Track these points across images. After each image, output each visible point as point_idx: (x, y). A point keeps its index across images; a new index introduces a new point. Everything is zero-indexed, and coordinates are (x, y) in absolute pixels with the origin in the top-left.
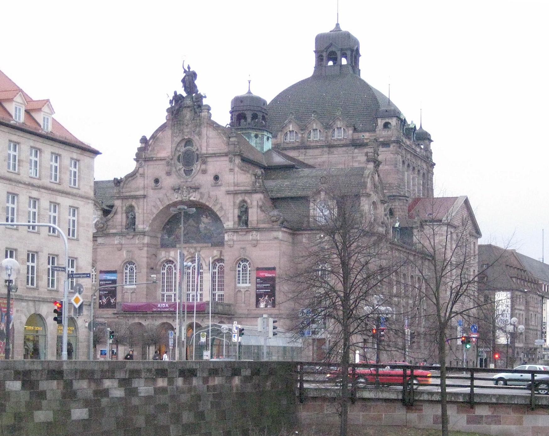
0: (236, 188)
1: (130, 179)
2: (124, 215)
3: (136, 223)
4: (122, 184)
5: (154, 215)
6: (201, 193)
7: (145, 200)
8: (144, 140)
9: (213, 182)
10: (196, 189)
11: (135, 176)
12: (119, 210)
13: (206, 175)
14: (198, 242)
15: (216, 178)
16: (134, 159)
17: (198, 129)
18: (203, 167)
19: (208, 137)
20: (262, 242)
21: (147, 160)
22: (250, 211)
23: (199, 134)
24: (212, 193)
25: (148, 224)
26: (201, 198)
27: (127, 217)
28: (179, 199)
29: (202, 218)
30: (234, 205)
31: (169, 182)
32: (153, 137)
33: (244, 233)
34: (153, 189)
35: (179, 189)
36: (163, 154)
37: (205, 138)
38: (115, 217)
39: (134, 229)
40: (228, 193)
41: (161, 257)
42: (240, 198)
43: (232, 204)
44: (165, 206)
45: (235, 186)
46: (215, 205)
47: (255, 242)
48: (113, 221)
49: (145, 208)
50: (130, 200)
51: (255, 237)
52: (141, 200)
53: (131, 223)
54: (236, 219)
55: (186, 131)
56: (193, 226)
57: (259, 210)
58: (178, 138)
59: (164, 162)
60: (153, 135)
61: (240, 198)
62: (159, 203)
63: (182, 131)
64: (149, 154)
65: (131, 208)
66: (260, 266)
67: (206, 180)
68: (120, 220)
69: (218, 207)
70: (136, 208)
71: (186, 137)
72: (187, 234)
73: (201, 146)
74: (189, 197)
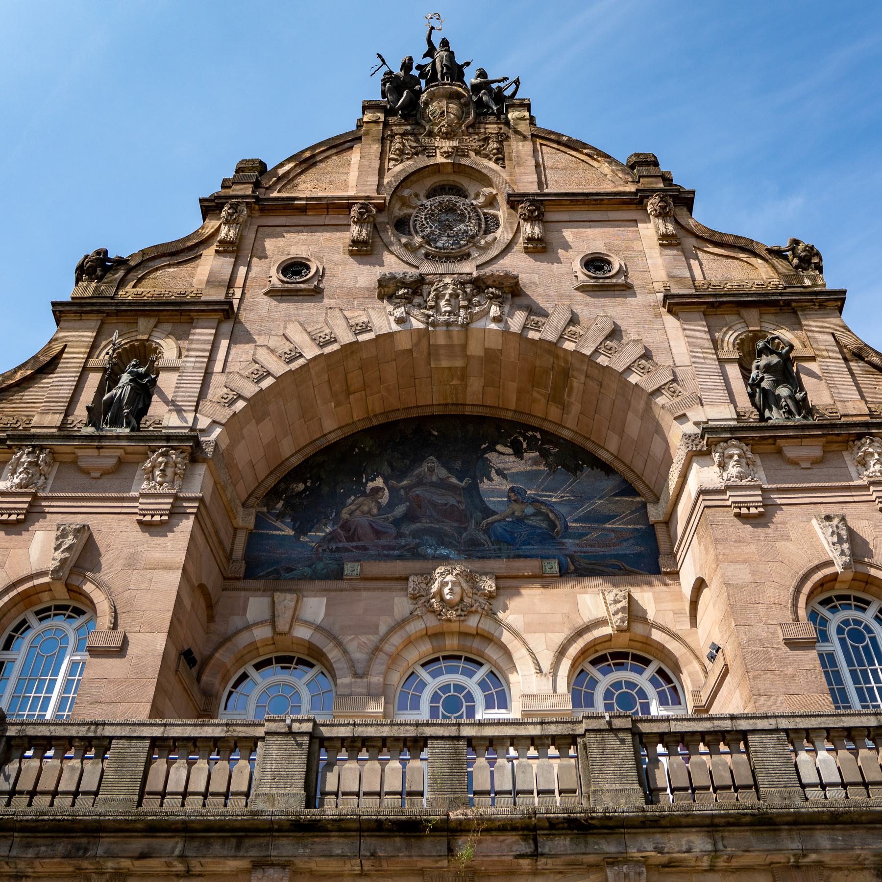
2: (94, 379)
12: (75, 357)
14: (471, 550)
24: (584, 314)
25: (224, 414)
33: (816, 451)
41: (237, 622)
49: (221, 354)
50: (144, 324)
56: (443, 484)
62: (300, 338)
68: (66, 392)
72: (410, 517)
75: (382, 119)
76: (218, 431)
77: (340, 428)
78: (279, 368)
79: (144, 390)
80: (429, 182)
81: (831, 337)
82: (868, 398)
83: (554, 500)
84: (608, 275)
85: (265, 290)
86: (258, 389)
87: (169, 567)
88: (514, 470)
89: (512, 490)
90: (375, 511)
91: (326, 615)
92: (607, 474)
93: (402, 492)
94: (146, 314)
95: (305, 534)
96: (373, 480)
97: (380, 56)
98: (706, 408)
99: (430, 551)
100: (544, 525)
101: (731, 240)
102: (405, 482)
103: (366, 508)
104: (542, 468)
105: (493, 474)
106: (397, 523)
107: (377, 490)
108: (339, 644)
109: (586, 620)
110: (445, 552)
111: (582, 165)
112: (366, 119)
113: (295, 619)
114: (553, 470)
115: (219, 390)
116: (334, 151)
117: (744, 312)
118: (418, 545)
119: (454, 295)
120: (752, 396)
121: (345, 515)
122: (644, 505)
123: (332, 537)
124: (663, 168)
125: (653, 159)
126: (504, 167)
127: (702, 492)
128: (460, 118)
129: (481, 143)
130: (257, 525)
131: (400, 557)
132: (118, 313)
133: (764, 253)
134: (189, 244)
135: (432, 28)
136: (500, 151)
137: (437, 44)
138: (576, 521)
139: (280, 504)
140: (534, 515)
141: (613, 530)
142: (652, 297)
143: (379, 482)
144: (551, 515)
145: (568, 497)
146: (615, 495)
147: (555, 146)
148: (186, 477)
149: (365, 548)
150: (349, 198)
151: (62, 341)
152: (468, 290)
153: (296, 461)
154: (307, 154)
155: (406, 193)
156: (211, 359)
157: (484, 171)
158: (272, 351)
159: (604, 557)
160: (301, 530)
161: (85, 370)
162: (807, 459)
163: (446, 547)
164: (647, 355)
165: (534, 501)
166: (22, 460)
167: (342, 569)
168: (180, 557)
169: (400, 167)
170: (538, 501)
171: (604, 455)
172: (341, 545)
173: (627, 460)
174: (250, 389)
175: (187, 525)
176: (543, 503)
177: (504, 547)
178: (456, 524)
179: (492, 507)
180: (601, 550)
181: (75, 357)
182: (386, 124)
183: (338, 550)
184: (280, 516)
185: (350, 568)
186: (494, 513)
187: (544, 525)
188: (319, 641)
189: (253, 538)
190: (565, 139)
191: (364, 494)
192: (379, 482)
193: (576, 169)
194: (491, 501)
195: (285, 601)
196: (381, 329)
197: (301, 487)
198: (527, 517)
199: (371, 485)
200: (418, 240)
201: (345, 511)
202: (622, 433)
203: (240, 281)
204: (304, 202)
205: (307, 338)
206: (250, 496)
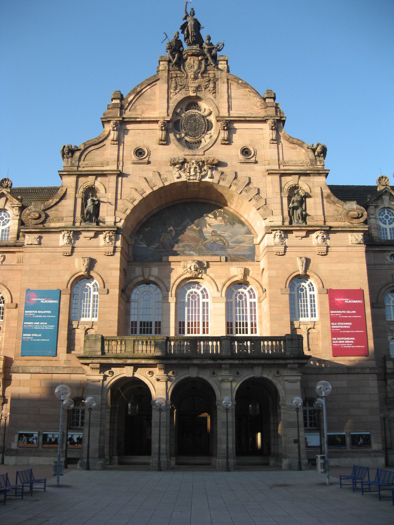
0: (282, 167)
2: (79, 201)
4: (77, 154)
7: (120, 179)
11: (101, 145)
19: (229, 97)
25: (124, 216)
27: (84, 205)
29: (207, 218)
33: (304, 234)
35: (183, 163)
38: (63, 202)
42: (290, 181)
53: (92, 215)
54: (286, 213)
58: (178, 95)
61: (290, 181)
62: (144, 185)
63: (185, 87)
65: (91, 191)
68: (72, 208)
75: (167, 69)
76: (123, 221)
77: (158, 207)
78: (139, 198)
79: (97, 207)
80: (186, 103)
82: (326, 214)
83: (225, 235)
84: (249, 157)
85: (130, 162)
86: (133, 206)
87: (116, 269)
88: (214, 224)
89: (213, 231)
90: (171, 238)
91: (158, 273)
92: (243, 226)
93: (179, 232)
95: (150, 247)
96: (170, 227)
98: (274, 216)
99: (187, 252)
100: (222, 244)
101: (295, 141)
102: (180, 228)
103: (168, 237)
104: (223, 223)
105: (207, 226)
107: (171, 231)
108: (163, 282)
109: (232, 275)
112: (160, 69)
113: (150, 275)
114: (226, 224)
115: (121, 206)
116: (149, 87)
118: (184, 250)
119: (195, 168)
120: (289, 212)
121: (161, 240)
122: (253, 238)
123: (158, 248)
124: (276, 102)
125: (273, 96)
127: (268, 246)
128: (199, 68)
129: (207, 83)
134: (100, 140)
136: (215, 88)
137: (189, 11)
138: (231, 243)
139: (141, 236)
140: (219, 240)
141: (243, 246)
142: (263, 167)
143: (171, 228)
144: (224, 241)
145: (230, 234)
146: (245, 234)
148: (116, 239)
149: (168, 251)
150: (157, 118)
151: (65, 186)
153: (145, 220)
154: (139, 89)
155: (179, 110)
156: (116, 193)
159: (239, 255)
161: (76, 199)
163: (192, 251)
164: (258, 193)
166: (65, 235)
167: (162, 259)
168: (118, 266)
169: (175, 97)
170: (221, 235)
171: (243, 219)
172: (161, 250)
173: (250, 222)
175: (118, 255)
176: (222, 236)
177: (210, 251)
178: (195, 243)
179: (206, 237)
180: (239, 253)
181: (71, 192)
182: (169, 71)
183: (160, 252)
184: (142, 240)
186: (207, 239)
187: (222, 244)
188: (157, 281)
190: (240, 82)
191: (167, 232)
192: (171, 228)
193: (243, 99)
194: (206, 235)
195: (147, 270)
196: (171, 181)
197: (147, 230)
199: (169, 229)
200: (183, 135)
201: (162, 238)
202: (248, 215)
203: (121, 158)
204: (140, 120)
206: (132, 233)
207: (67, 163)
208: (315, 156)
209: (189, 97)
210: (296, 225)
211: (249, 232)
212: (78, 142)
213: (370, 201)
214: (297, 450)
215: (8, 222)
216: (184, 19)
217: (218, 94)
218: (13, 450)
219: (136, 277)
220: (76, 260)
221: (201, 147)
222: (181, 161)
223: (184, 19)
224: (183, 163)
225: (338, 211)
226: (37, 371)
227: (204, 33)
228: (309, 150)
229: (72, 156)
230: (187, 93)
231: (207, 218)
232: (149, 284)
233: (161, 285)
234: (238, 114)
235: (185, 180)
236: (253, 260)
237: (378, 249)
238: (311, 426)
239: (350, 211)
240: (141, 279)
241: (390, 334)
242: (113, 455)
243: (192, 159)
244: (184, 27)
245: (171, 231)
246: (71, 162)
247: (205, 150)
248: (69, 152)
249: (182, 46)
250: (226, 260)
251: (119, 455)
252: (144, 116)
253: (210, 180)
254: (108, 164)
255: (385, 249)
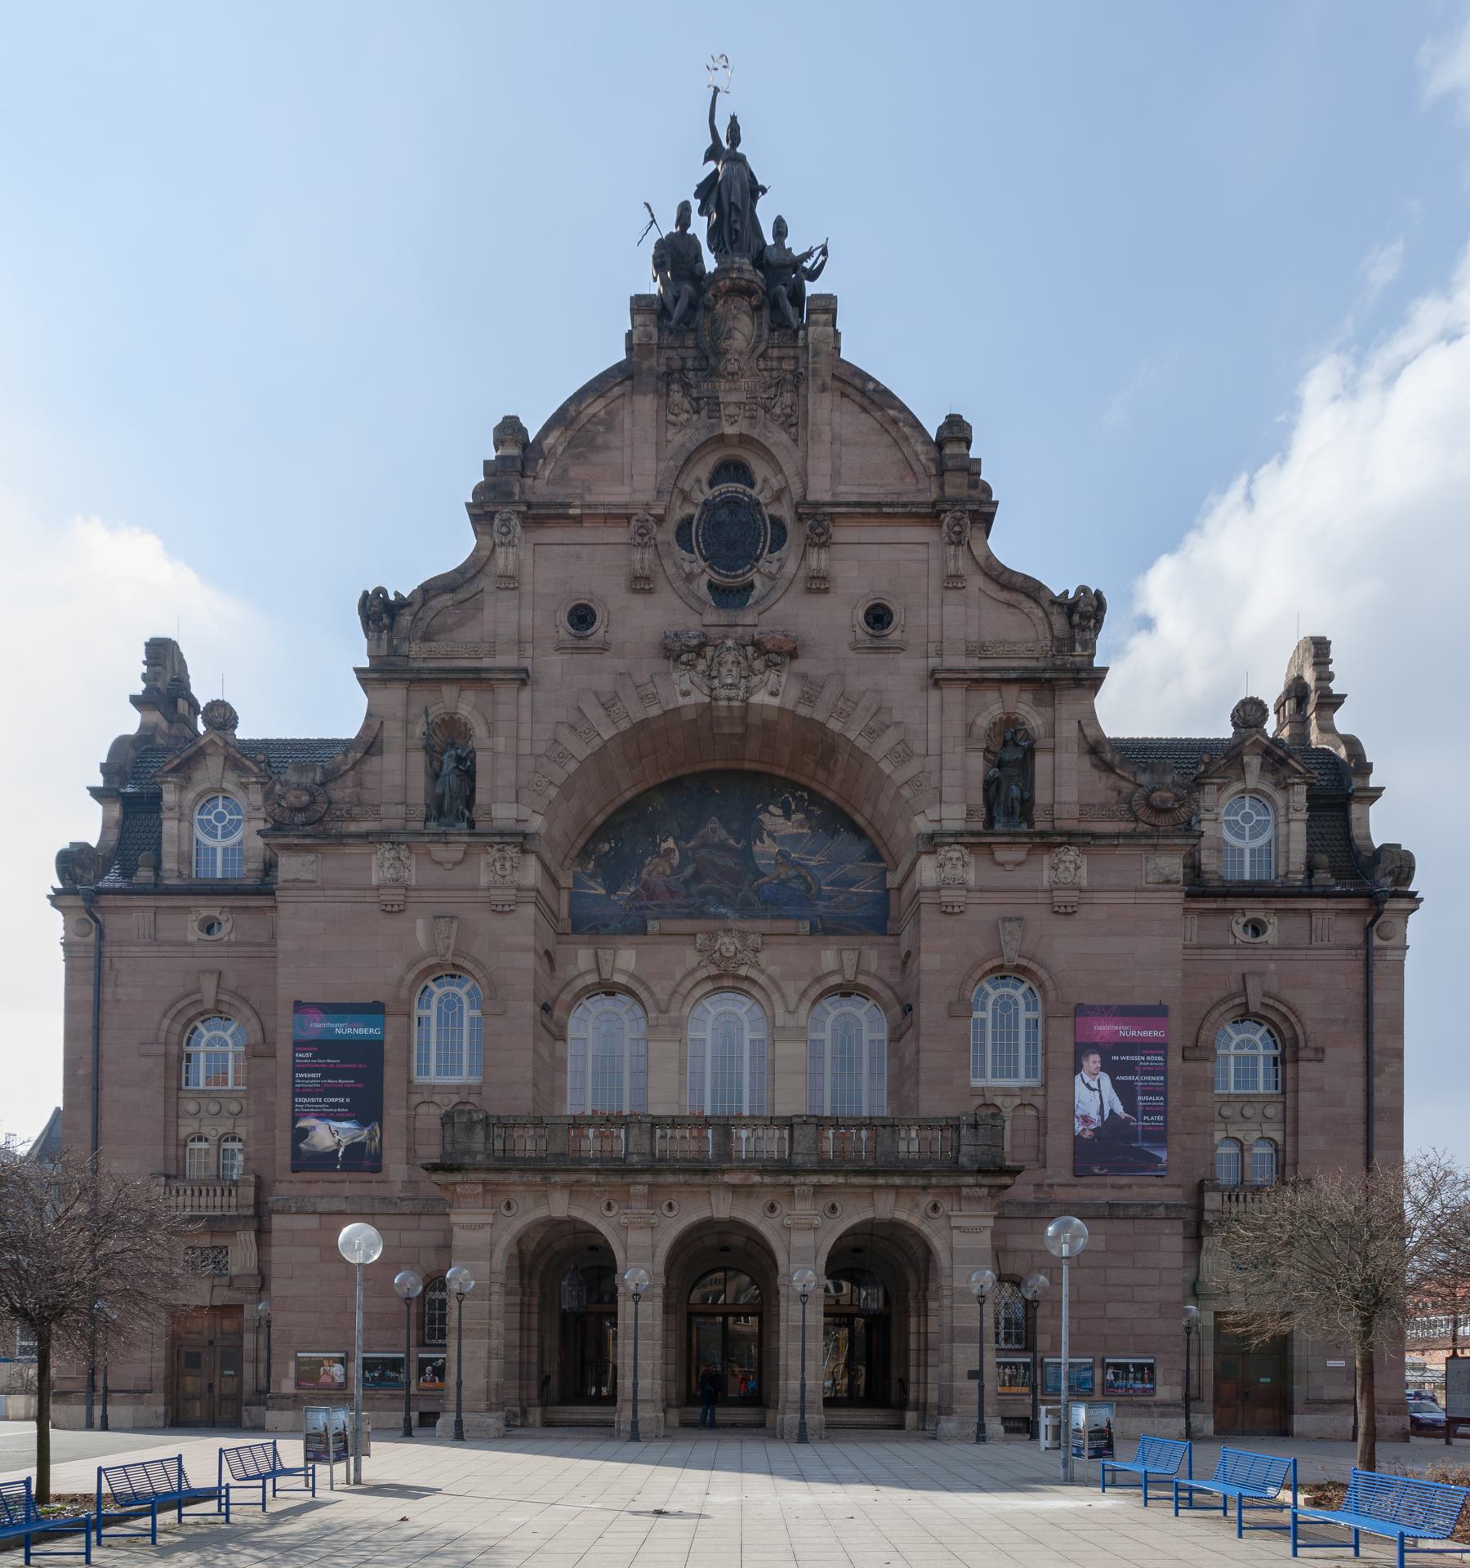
1: (446, 599)
3: (481, 797)
4: (405, 619)
5: (572, 766)
6: (804, 677)
7: (526, 695)
8: (509, 430)
9: (862, 632)
10: (779, 653)
13: (823, 600)
15: (878, 617)
16: (468, 505)
17: (787, 398)
18: (818, 559)
20: (1100, 897)
21: (538, 516)
22: (1042, 762)
23: (794, 422)
26: (808, 699)
28: (699, 697)
30: (969, 733)
31: (637, 622)
32: (560, 419)
34: (560, 649)
35: (699, 650)
36: (613, 494)
37: (827, 437)
38: (374, 763)
39: (472, 824)
40: (936, 680)
42: (991, 707)
43: (959, 730)
44: (625, 725)
45: (969, 653)
46: (873, 733)
47: (1071, 896)
48: (359, 784)
50: (448, 692)
51: (1066, 876)
52: (506, 693)
54: (977, 798)
55: (730, 395)
57: (1086, 761)
58: (689, 431)
59: (619, 534)
60: (563, 409)
61: (991, 707)
62: (594, 713)
64: (541, 486)
66: (1089, 999)
67: (828, 622)
69: (889, 739)
70: (480, 731)
71: (729, 430)
73: (803, 475)
74: (749, 691)
75: (655, 340)
78: (580, 749)
81: (1076, 725)
94: (447, 681)
97: (647, 205)
106: (686, 883)
110: (723, 910)
111: (886, 439)
117: (1005, 688)
126: (795, 441)
130: (575, 885)
131: (689, 916)
132: (421, 681)
133: (1046, 604)
135: (716, 90)
147: (858, 398)
150: (626, 506)
152: (749, 654)
155: (687, 483)
157: (773, 450)
158: (573, 728)
160: (611, 889)
162: (1010, 863)
165: (796, 864)
174: (560, 776)
185: (653, 926)
189: (574, 897)
190: (871, 386)
198: (789, 879)
204: (578, 511)
205: (601, 711)
207: (378, 646)
208: (1072, 626)
209: (723, 435)
210: (1005, 830)
211: (875, 855)
212: (403, 584)
213: (1205, 771)
214: (976, 1397)
215: (236, 828)
216: (706, 160)
217: (806, 427)
218: (286, 1397)
219: (581, 975)
220: (420, 923)
221: (751, 601)
222: (694, 642)
223: (706, 160)
224: (699, 650)
225: (1120, 792)
226: (335, 1208)
227: (765, 213)
228: (1055, 609)
229: (390, 628)
230: (713, 425)
231: (764, 817)
232: (612, 994)
233: (644, 996)
234: (860, 494)
235: (707, 699)
236: (883, 931)
237: (1214, 906)
238: (1006, 1341)
239: (1154, 790)
240: (591, 979)
241: (1222, 1126)
242: (530, 1405)
243: (727, 637)
244: (708, 190)
245: (669, 851)
246: (390, 640)
247: (761, 608)
248: (378, 611)
249: (698, 257)
250: (814, 931)
251: (544, 1403)
252: (590, 498)
253: (775, 701)
254: (492, 653)
255: (1231, 904)
